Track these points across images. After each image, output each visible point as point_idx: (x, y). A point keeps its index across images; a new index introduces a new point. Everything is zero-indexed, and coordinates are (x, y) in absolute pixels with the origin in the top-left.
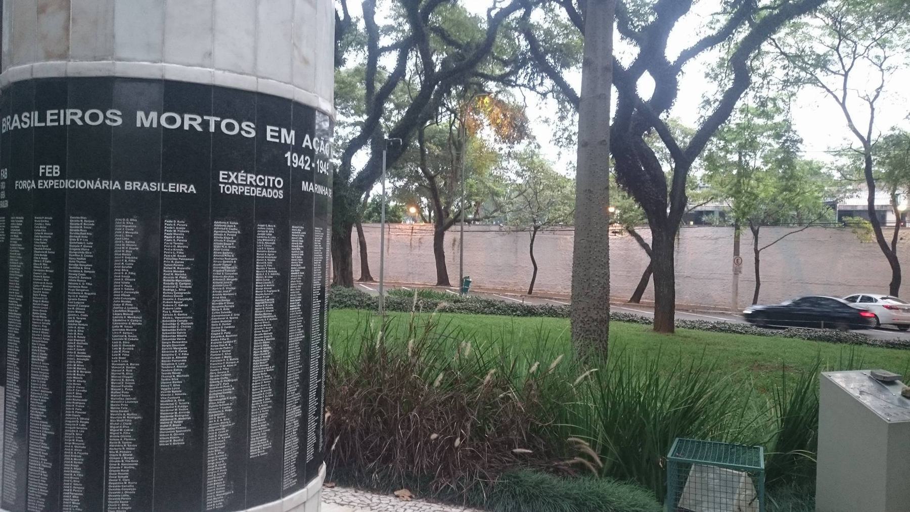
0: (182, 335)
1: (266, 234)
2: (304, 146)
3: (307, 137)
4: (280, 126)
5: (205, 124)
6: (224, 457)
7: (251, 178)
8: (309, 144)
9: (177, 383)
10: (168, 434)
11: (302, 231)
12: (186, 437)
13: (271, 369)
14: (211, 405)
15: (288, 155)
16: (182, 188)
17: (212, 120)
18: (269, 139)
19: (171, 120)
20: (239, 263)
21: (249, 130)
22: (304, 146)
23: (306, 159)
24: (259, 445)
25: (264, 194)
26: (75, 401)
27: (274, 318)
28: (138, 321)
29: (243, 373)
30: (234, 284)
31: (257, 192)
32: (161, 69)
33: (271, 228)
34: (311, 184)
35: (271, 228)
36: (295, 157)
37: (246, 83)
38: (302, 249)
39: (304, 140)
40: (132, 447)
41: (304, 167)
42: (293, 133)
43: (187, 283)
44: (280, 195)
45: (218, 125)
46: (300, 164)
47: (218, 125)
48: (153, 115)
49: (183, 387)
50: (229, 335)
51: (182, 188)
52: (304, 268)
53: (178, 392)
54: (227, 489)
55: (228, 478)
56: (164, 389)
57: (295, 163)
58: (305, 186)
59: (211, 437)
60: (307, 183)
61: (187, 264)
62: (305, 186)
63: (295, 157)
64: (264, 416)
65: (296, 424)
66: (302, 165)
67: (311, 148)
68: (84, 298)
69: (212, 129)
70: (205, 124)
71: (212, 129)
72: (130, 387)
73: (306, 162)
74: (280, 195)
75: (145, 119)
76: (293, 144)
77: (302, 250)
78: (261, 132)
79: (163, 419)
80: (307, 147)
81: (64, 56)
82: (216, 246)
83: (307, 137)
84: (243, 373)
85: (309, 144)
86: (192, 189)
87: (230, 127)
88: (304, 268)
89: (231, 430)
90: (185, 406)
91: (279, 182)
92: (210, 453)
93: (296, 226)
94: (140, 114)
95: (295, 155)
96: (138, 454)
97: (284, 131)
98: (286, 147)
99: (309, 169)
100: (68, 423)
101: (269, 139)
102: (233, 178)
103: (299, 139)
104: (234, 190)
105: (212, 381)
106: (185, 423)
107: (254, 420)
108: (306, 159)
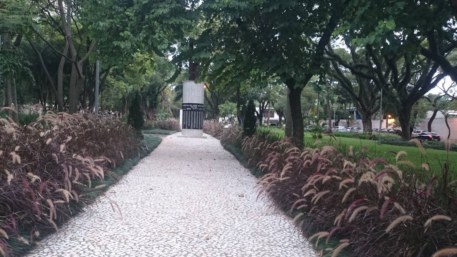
24: (189, 125)
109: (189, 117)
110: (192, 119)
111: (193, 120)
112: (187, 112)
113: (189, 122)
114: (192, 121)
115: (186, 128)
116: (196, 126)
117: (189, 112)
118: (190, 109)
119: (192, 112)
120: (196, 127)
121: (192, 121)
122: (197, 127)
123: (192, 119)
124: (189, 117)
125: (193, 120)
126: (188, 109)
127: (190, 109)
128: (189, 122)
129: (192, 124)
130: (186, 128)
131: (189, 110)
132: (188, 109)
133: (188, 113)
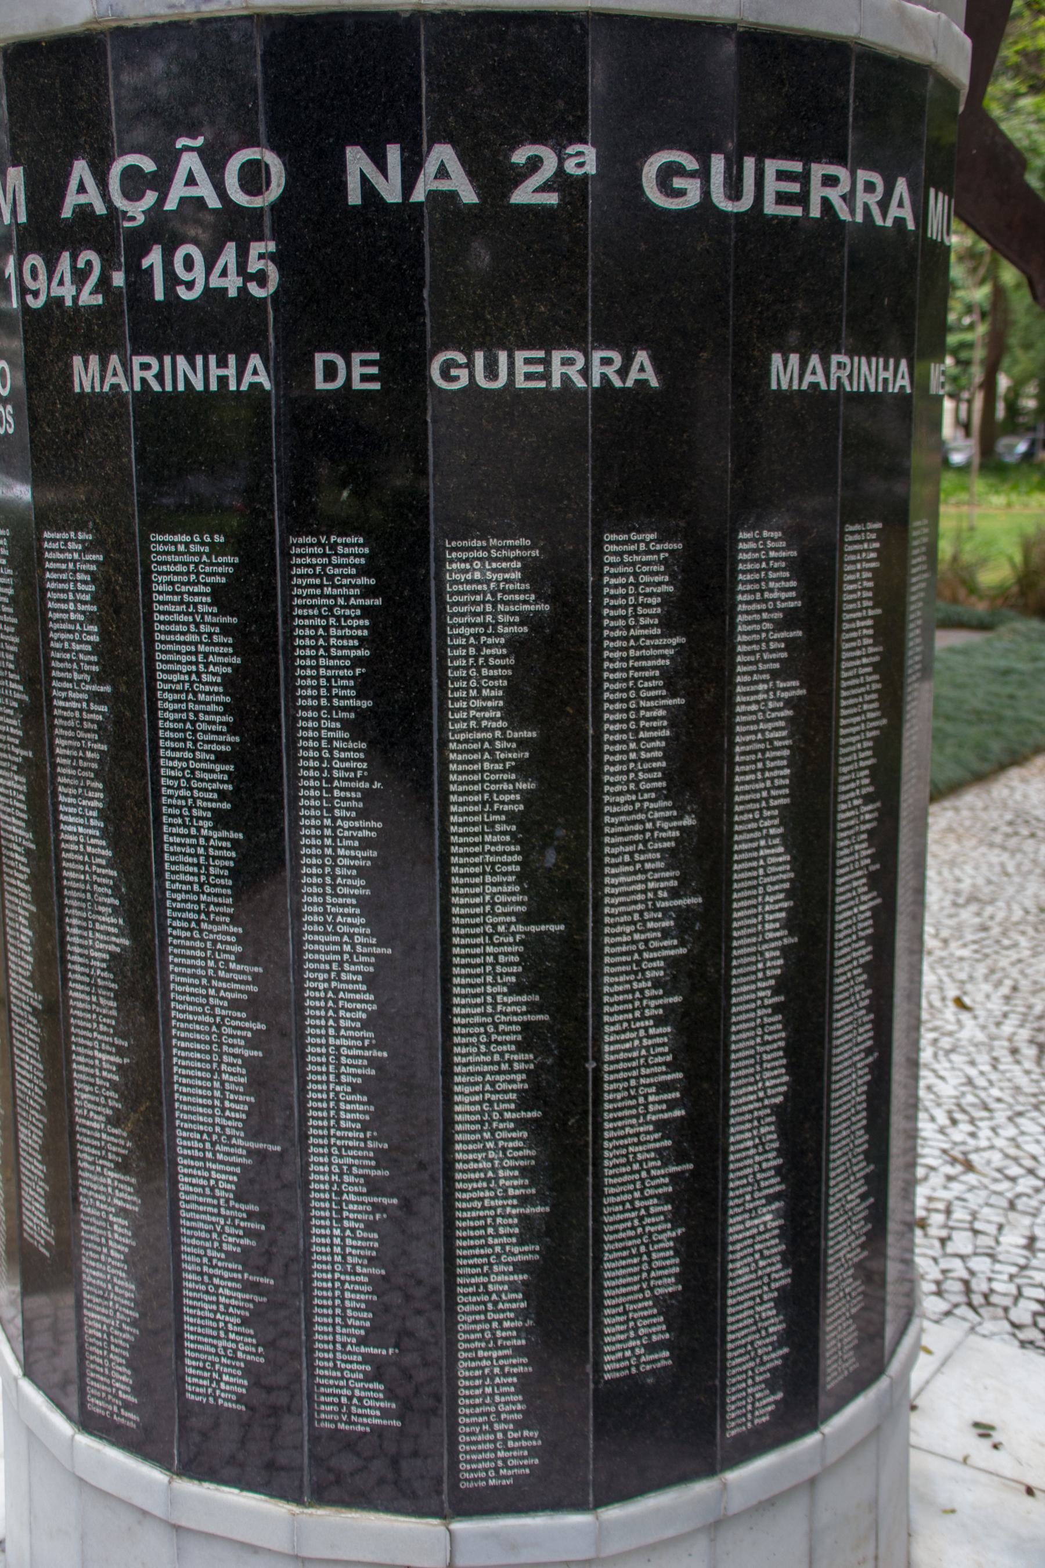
2: (67, 213)
3: (80, 169)
8: (93, 197)
11: (86, 550)
22: (67, 213)
23: (81, 265)
34: (114, 360)
36: (34, 268)
38: (90, 618)
39: (66, 185)
41: (75, 299)
46: (56, 291)
52: (108, 689)
57: (36, 294)
60: (94, 360)
63: (34, 268)
66: (67, 292)
67: (100, 209)
73: (80, 276)
76: (22, 218)
77: (91, 622)
80: (84, 212)
83: (80, 169)
85: (93, 197)
88: (108, 689)
93: (59, 530)
95: (34, 259)
99: (99, 299)
108: (81, 265)
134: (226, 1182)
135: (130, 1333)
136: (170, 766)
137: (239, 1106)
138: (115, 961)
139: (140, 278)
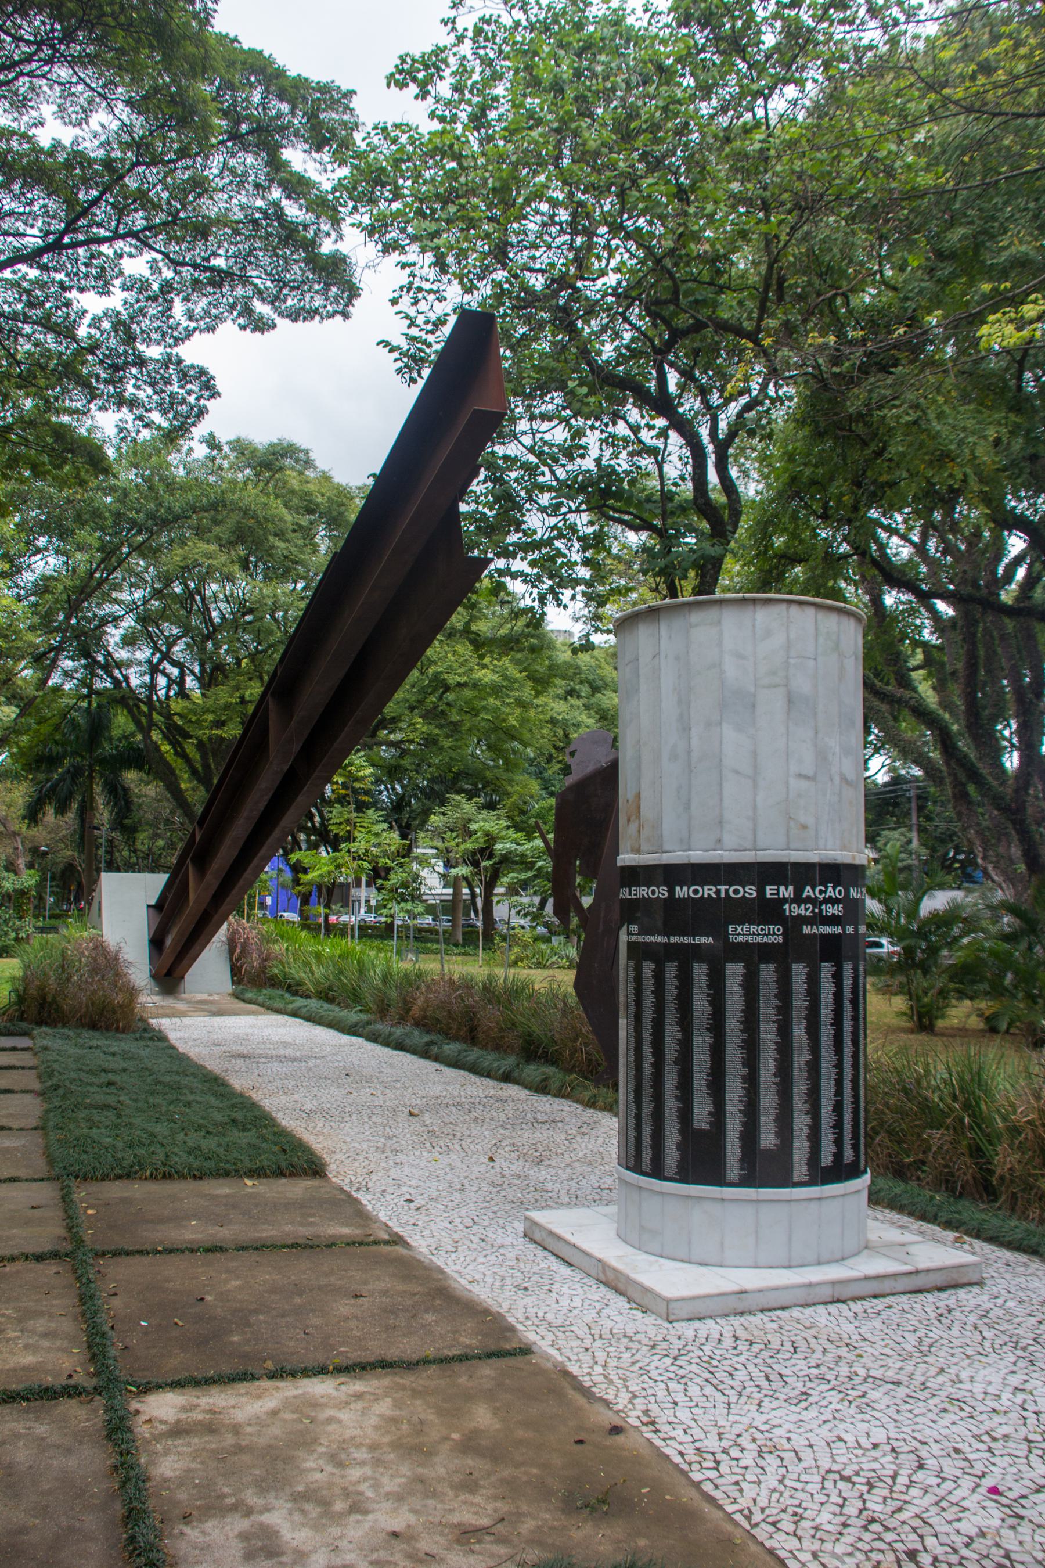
0: (707, 1048)
1: (768, 972)
3: (808, 888)
4: (779, 884)
5: (718, 892)
6: (738, 1143)
7: (753, 928)
9: (704, 1083)
10: (699, 1121)
12: (711, 1123)
13: (777, 1080)
14: (728, 1102)
15: (787, 906)
16: (704, 940)
17: (723, 888)
18: (768, 896)
19: (696, 892)
20: (745, 995)
21: (751, 891)
24: (768, 1139)
25: (765, 939)
26: (647, 1091)
27: (778, 1039)
28: (679, 1035)
29: (752, 1081)
30: (743, 1011)
31: (759, 939)
32: (688, 856)
33: (772, 967)
35: (772, 967)
37: (748, 857)
40: (678, 1127)
42: (791, 888)
43: (709, 1010)
44: (780, 939)
45: (727, 891)
47: (727, 891)
48: (685, 888)
49: (708, 1086)
50: (740, 1050)
51: (704, 940)
53: (705, 1090)
54: (742, 1169)
55: (742, 1160)
56: (696, 1086)
58: (807, 930)
59: (729, 1127)
61: (708, 995)
62: (807, 930)
64: (772, 1117)
65: (806, 1130)
66: (803, 913)
68: (650, 1018)
69: (723, 895)
70: (718, 892)
71: (723, 895)
72: (675, 1083)
74: (780, 939)
75: (681, 892)
78: (761, 892)
79: (696, 1109)
81: (638, 851)
82: (728, 982)
83: (808, 888)
84: (752, 1081)
86: (711, 940)
87: (736, 892)
89: (744, 1124)
90: (709, 1101)
91: (778, 929)
92: (728, 1139)
94: (678, 889)
96: (681, 1131)
97: (782, 888)
98: (785, 900)
100: (644, 1106)
101: (768, 896)
102: (739, 930)
103: (799, 891)
104: (740, 939)
105: (727, 1084)
106: (710, 1113)
107: (763, 1119)
109: (768, 1034)
110: (801, 1058)
111: (814, 1068)
112: (735, 972)
113: (768, 1101)
114: (800, 1088)
115: (733, 1168)
116: (838, 1142)
117: (768, 972)
118: (773, 934)
119: (799, 972)
120: (838, 1155)
121: (800, 1088)
122: (848, 1154)
123: (801, 1058)
124: (768, 1034)
125: (814, 1068)
126: (743, 933)
127: (773, 934)
128: (768, 1101)
129: (801, 1122)
130: (733, 1168)
131: (765, 952)
132: (743, 933)
133: (751, 986)
134: (830, 1109)
135: (807, 1155)
136: (823, 1013)
137: (833, 1091)
138: (807, 1063)
139: (821, 910)
